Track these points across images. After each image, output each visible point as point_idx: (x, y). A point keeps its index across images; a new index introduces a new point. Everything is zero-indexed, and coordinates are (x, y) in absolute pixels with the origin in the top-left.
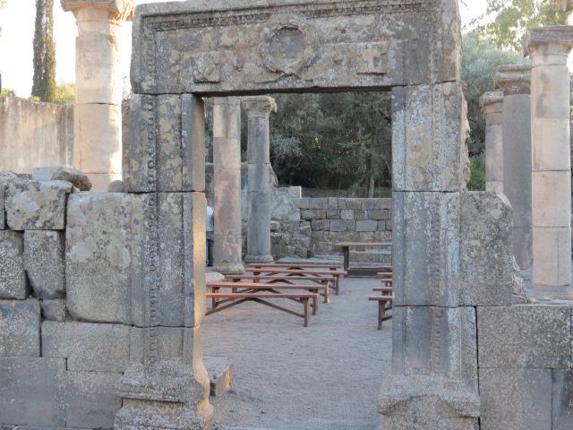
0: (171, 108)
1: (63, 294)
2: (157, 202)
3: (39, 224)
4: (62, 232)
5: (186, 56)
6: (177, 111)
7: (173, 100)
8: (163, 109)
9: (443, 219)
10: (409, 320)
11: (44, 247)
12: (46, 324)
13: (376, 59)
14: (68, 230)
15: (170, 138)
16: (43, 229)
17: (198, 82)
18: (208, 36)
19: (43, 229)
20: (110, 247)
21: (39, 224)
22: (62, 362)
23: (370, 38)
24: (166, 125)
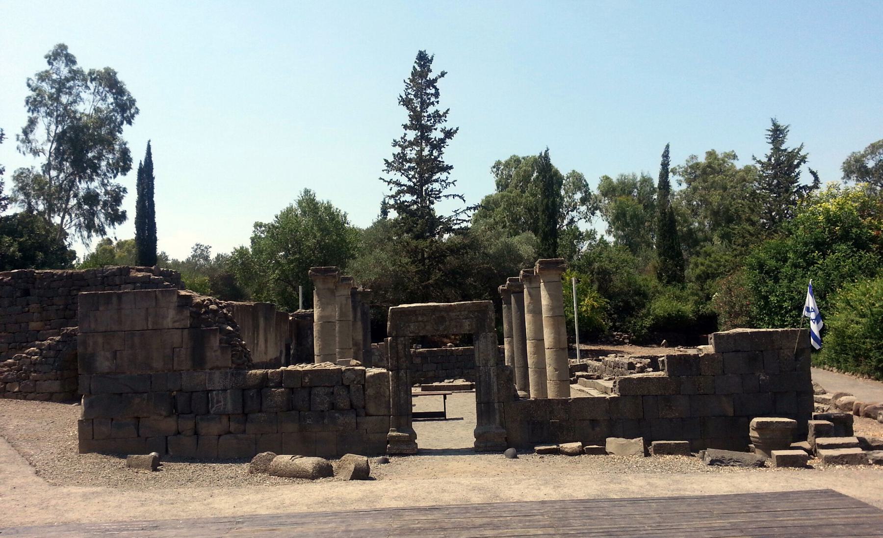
0: (402, 341)
1: (364, 407)
2: (398, 373)
3: (355, 382)
4: (363, 385)
5: (407, 324)
6: (404, 342)
7: (402, 339)
8: (399, 342)
9: (492, 375)
10: (483, 408)
11: (358, 390)
12: (358, 418)
13: (469, 325)
14: (366, 384)
15: (402, 351)
16: (357, 384)
17: (410, 333)
18: (414, 318)
19: (357, 384)
20: (382, 389)
21: (355, 382)
22: (365, 431)
23: (466, 318)
24: (400, 347)
